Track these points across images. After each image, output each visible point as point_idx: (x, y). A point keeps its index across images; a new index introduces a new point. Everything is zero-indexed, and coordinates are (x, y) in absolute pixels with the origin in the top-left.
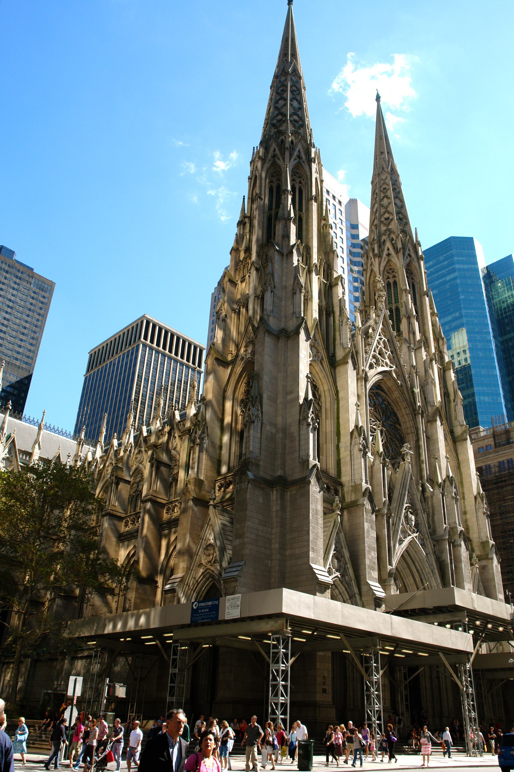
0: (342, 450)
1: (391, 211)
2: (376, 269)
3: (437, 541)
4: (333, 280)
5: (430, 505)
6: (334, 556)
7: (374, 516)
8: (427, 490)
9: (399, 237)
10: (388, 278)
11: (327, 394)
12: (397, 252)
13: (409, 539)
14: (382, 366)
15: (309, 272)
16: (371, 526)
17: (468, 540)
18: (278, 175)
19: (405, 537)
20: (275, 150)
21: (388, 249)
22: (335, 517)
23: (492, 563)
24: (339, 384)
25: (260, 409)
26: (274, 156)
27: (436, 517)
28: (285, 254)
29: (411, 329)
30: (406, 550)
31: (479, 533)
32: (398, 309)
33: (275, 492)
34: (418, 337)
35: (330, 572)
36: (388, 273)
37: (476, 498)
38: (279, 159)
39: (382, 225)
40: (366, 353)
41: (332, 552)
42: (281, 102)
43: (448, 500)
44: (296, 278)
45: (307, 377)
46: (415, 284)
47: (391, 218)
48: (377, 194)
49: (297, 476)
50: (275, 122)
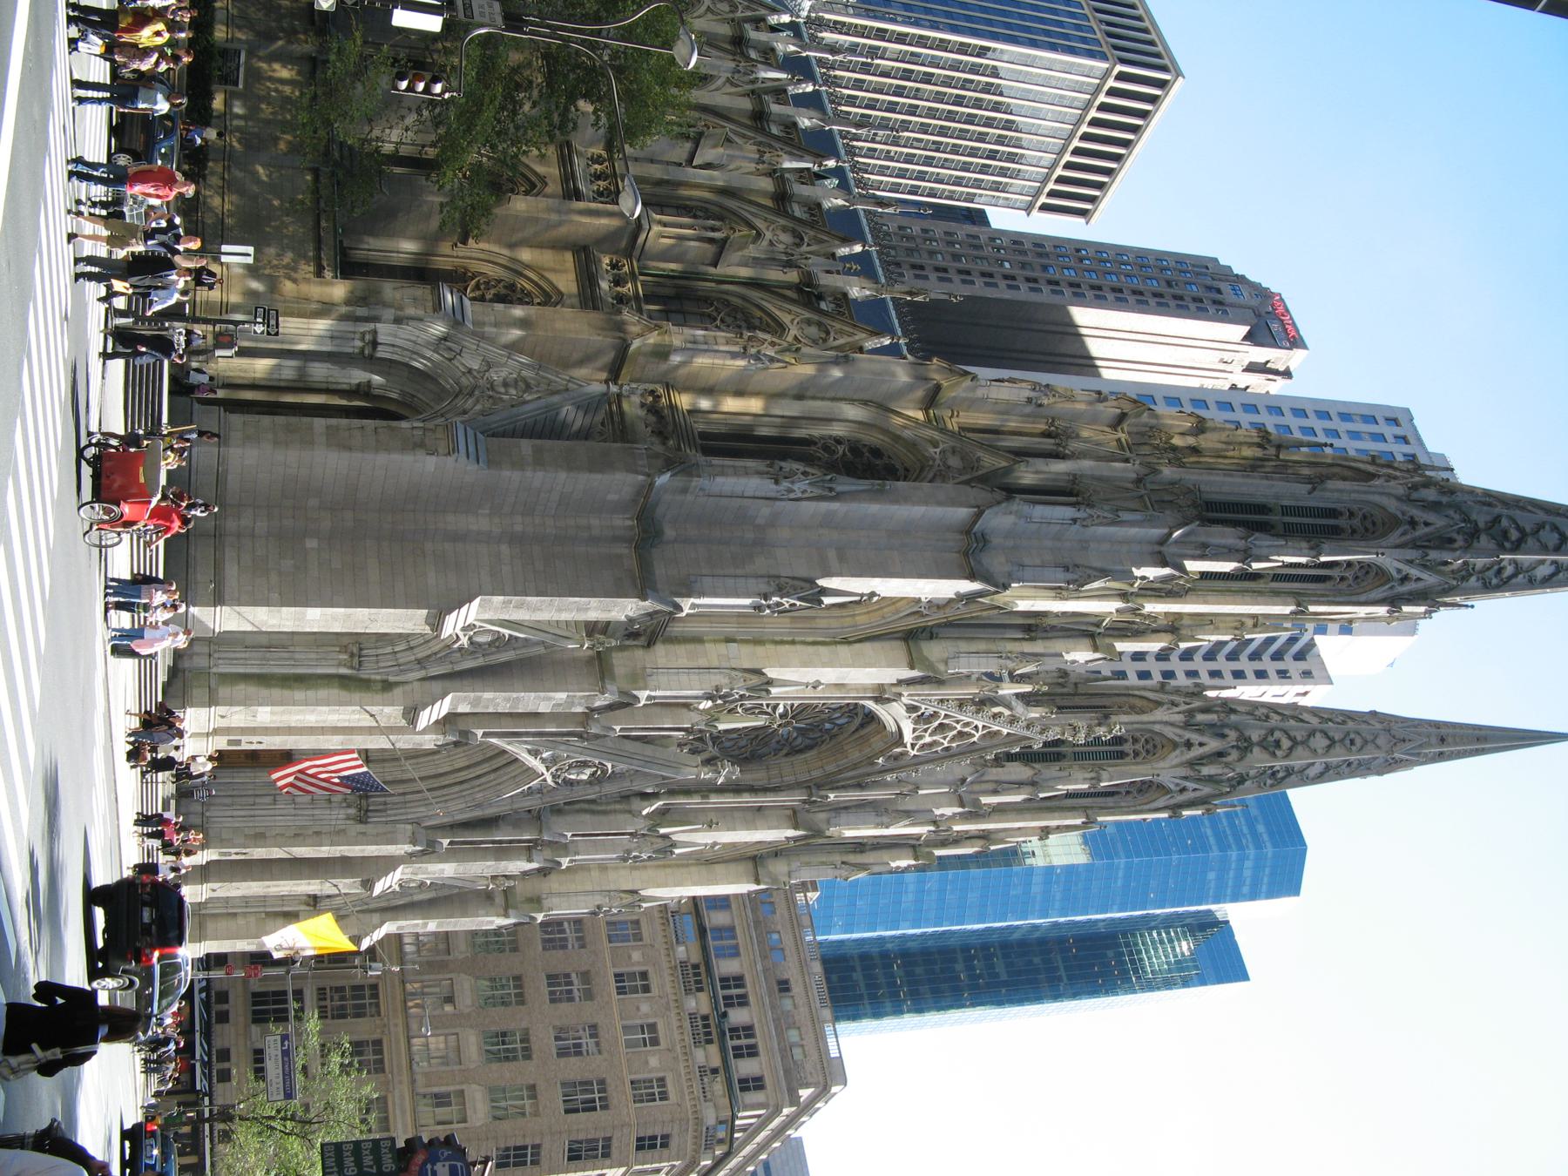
0: (722, 648)
1: (1294, 753)
2: (1160, 714)
3: (536, 818)
4: (1108, 640)
5: (612, 807)
6: (500, 637)
7: (579, 709)
8: (646, 803)
9: (1226, 770)
11: (848, 621)
12: (1191, 764)
13: (541, 768)
14: (914, 730)
15: (1124, 596)
16: (560, 705)
17: (543, 872)
18: (1367, 530)
19: (543, 761)
20: (1427, 524)
21: (1201, 745)
22: (578, 637)
24: (867, 647)
25: (806, 495)
26: (1413, 523)
27: (587, 817)
28: (1162, 549)
29: (1006, 786)
30: (517, 759)
31: (560, 894)
33: (629, 523)
34: (985, 800)
36: (1147, 741)
37: (634, 892)
38: (1403, 534)
39: (1263, 732)
42: (1551, 539)
43: (625, 842)
44: (1103, 573)
45: (873, 594)
46: (1116, 798)
47: (1279, 753)
48: (1344, 722)
49: (660, 571)
50: (1505, 523)
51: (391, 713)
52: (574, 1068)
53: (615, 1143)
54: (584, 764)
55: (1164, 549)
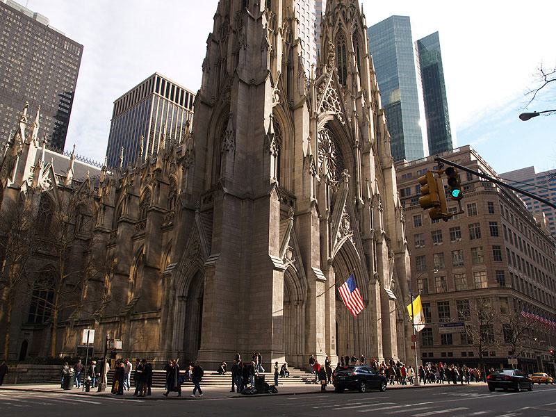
0: (296, 173)
3: (365, 242)
10: (339, 43)
11: (287, 130)
12: (347, 23)
15: (276, 35)
17: (388, 240)
19: (342, 237)
21: (340, 20)
23: (404, 256)
32: (345, 68)
34: (359, 90)
35: (285, 261)
40: (318, 100)
41: (287, 246)
43: (375, 211)
51: (320, 288)
52: (465, 235)
53: (491, 221)
54: (343, 223)
55: (256, 19)
